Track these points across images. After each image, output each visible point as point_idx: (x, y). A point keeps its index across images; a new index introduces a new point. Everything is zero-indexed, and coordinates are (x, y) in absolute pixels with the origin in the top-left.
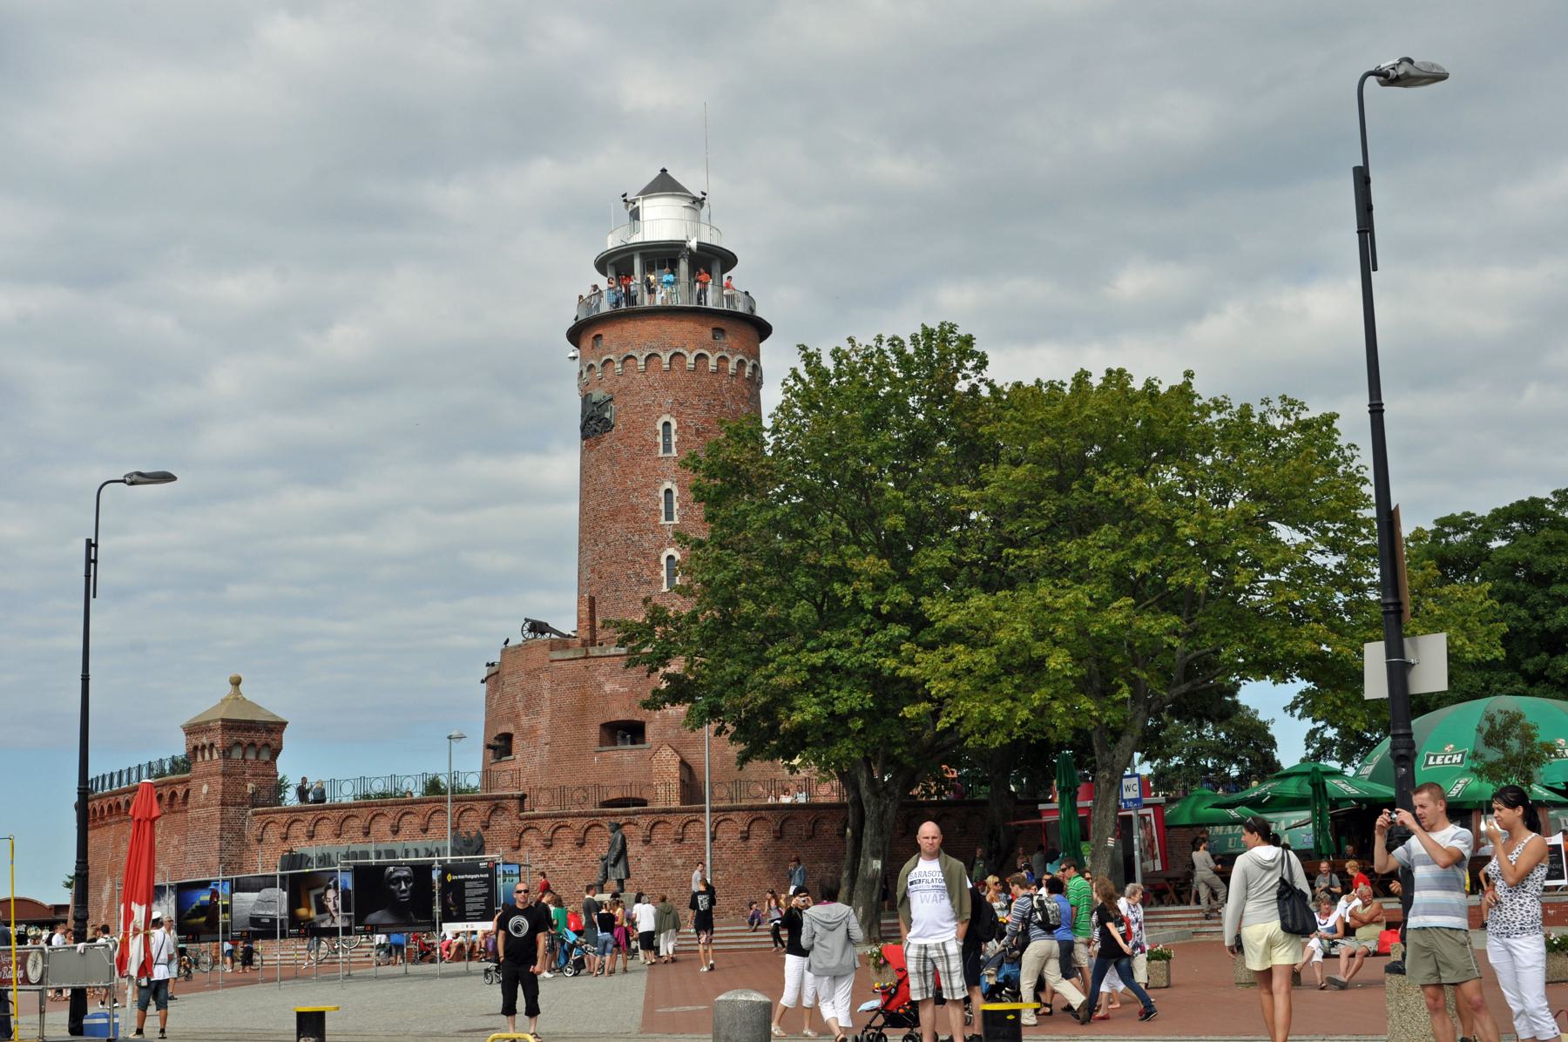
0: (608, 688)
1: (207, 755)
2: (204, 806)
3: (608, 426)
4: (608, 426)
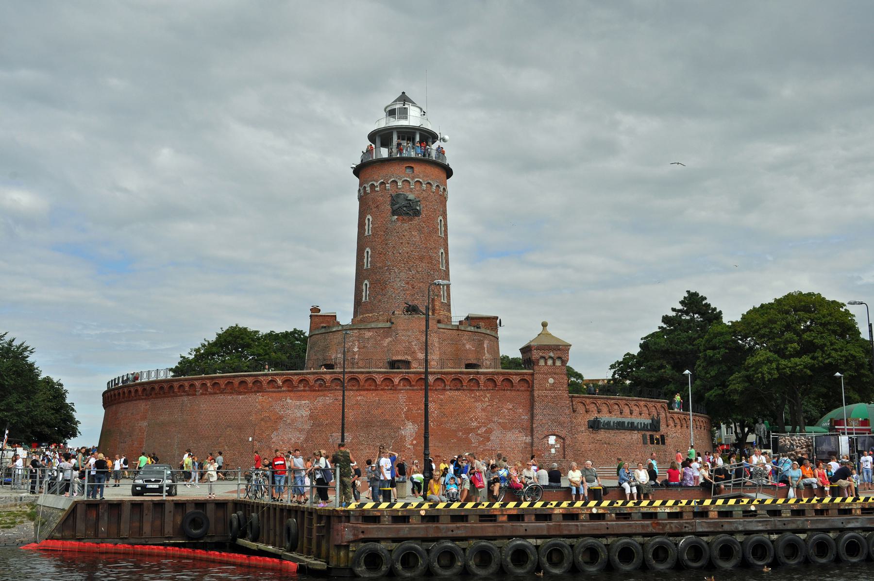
0: (468, 346)
1: (550, 362)
2: (551, 390)
3: (417, 213)
4: (417, 213)
